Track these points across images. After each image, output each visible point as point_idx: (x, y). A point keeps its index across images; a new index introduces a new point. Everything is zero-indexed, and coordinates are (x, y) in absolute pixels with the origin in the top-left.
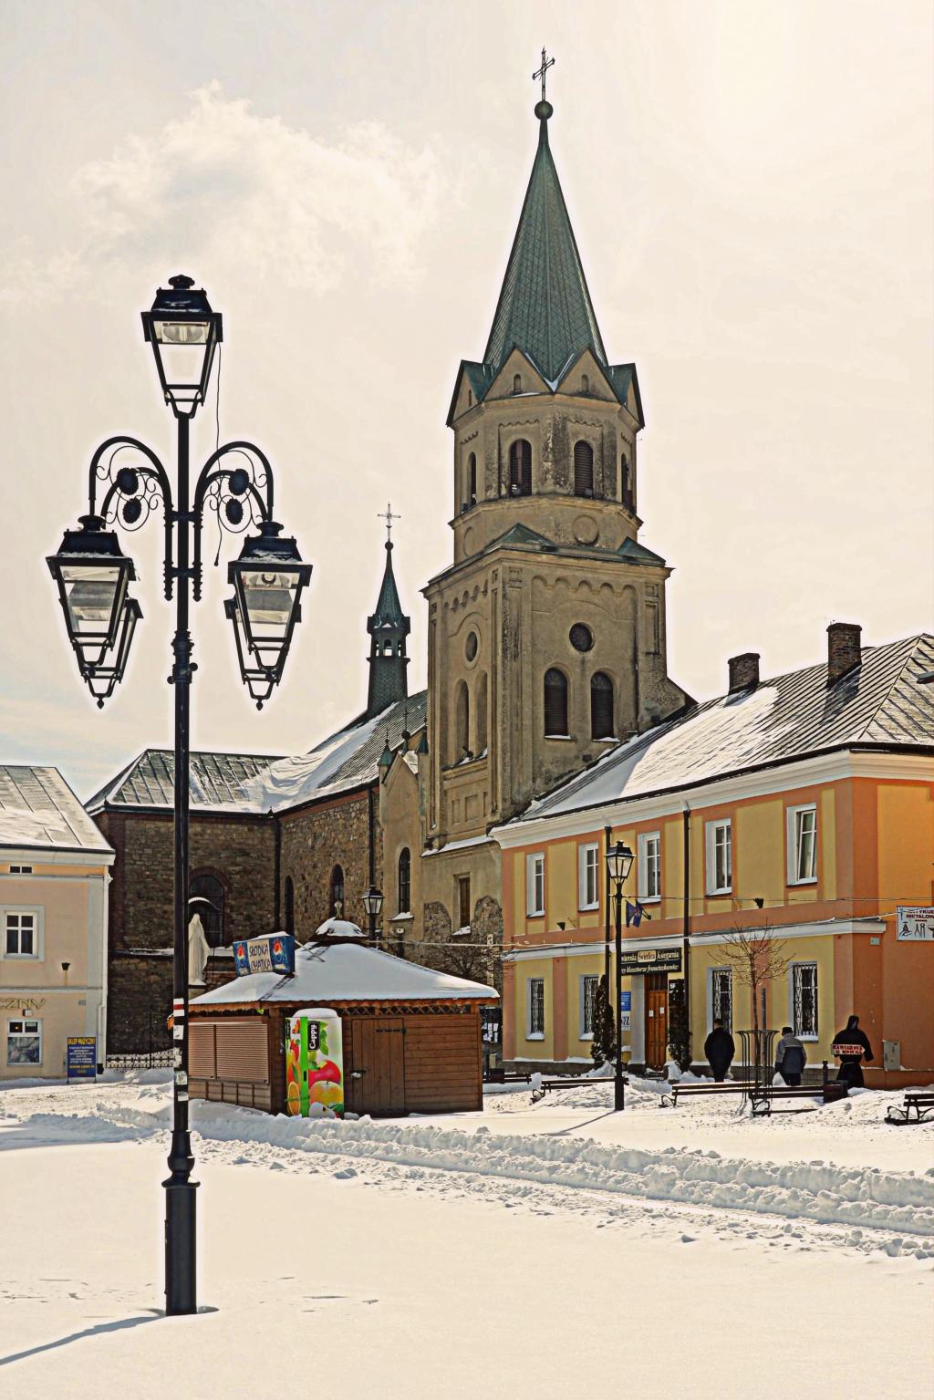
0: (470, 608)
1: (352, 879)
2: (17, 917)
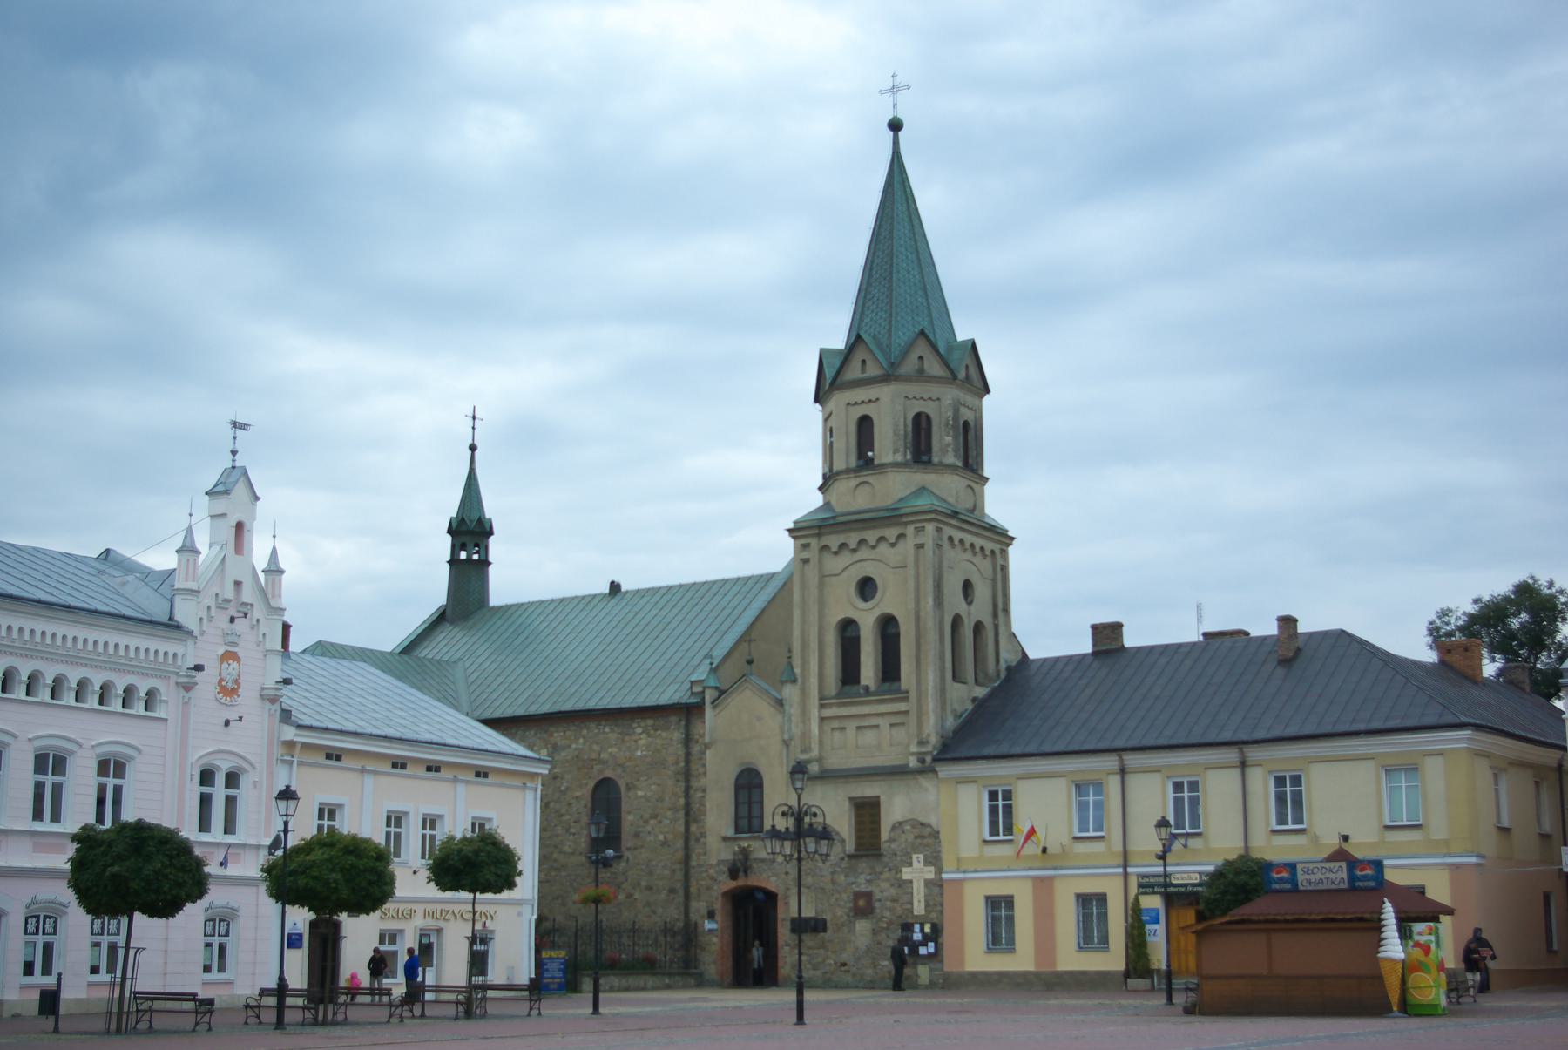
0: (864, 553)
2: (334, 820)
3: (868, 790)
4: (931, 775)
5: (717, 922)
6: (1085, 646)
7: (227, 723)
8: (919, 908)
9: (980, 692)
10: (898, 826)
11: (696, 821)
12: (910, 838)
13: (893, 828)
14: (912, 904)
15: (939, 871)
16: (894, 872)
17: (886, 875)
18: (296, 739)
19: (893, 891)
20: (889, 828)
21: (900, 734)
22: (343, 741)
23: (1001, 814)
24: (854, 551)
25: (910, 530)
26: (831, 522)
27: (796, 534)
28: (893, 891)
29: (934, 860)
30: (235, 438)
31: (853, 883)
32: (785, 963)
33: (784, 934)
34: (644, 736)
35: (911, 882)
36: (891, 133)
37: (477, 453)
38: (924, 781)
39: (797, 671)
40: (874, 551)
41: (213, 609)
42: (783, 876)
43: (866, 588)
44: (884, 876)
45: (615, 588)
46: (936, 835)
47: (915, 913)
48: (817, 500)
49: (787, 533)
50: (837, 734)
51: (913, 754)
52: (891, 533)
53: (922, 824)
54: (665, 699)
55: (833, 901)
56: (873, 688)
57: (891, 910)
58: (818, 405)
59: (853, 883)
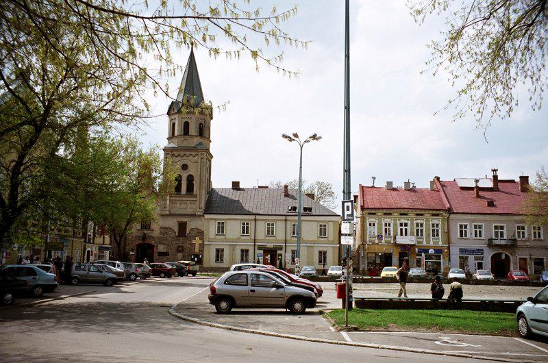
0: (185, 157)
3: (184, 220)
8: (197, 250)
10: (192, 229)
23: (221, 229)
25: (200, 153)
29: (202, 238)
43: (185, 167)
52: (194, 153)
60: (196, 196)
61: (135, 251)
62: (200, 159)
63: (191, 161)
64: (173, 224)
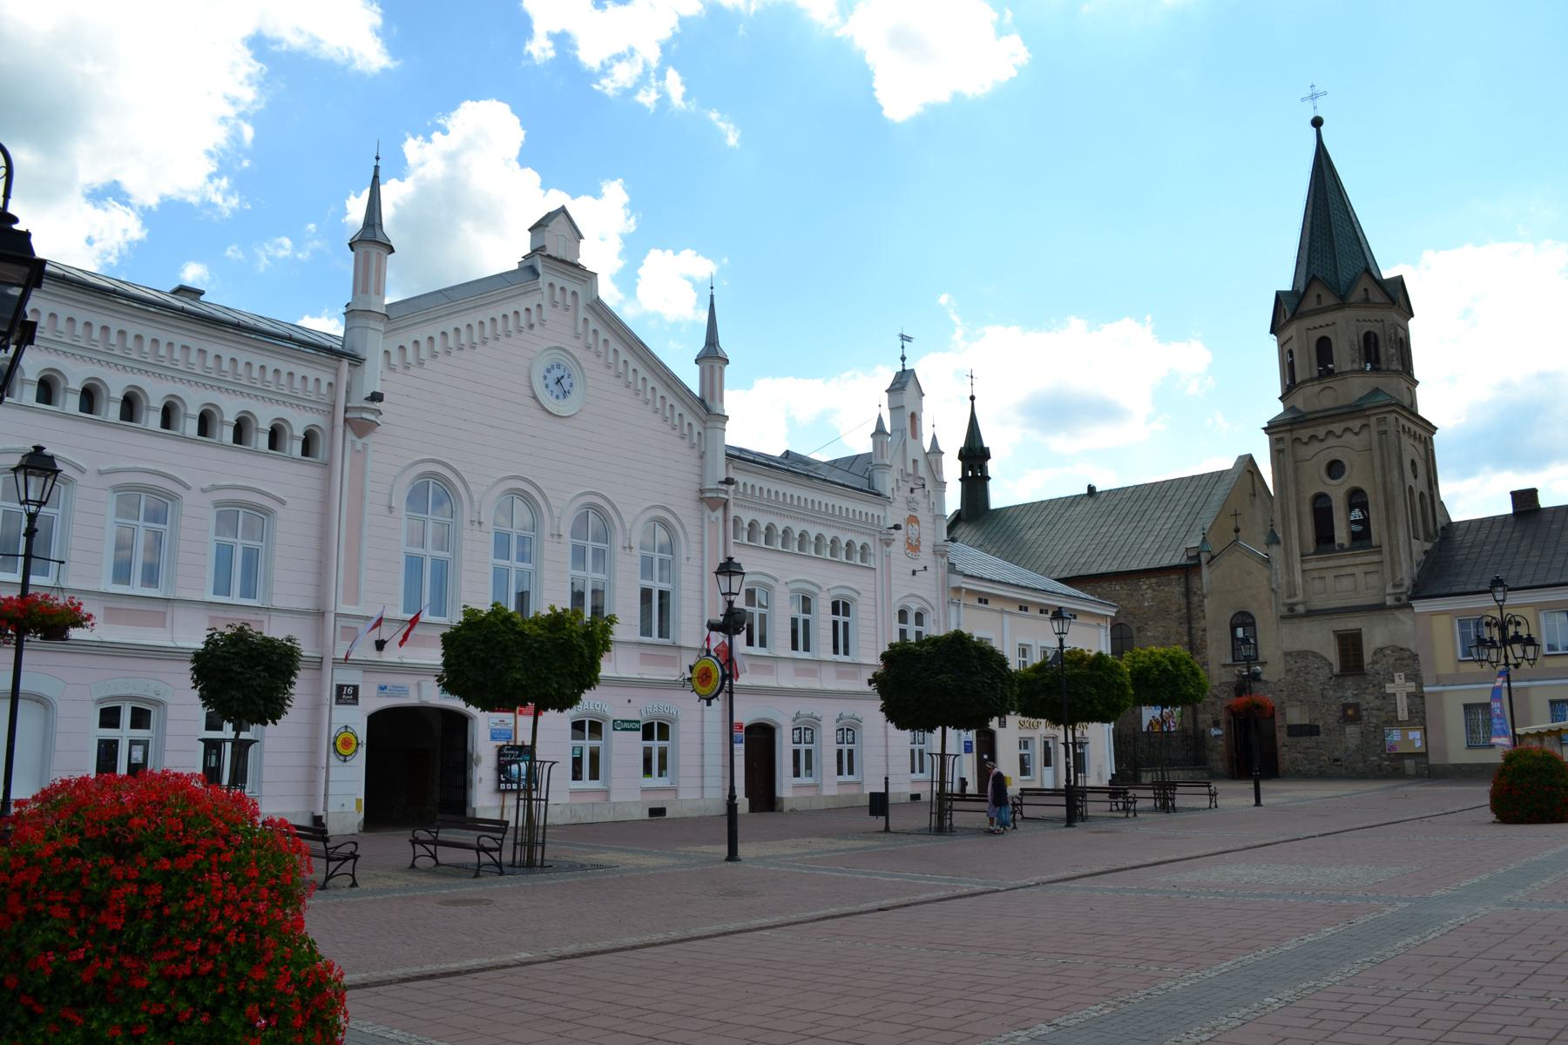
0: (1332, 441)
1: (1149, 634)
3: (1349, 624)
4: (1407, 610)
5: (1222, 729)
6: (1507, 508)
7: (914, 573)
8: (1403, 714)
9: (1428, 546)
11: (1198, 654)
12: (1392, 661)
13: (1375, 654)
14: (1396, 712)
15: (1420, 686)
16: (1377, 688)
17: (1371, 690)
18: (963, 586)
19: (1378, 703)
20: (1371, 653)
21: (1374, 580)
22: (992, 588)
24: (1322, 440)
25: (1373, 420)
26: (1302, 419)
27: (1269, 431)
28: (1378, 703)
29: (1415, 677)
30: (903, 347)
31: (1341, 697)
32: (1285, 759)
33: (1282, 736)
34: (1149, 591)
35: (1394, 694)
36: (1315, 129)
37: (975, 401)
38: (1399, 614)
39: (1280, 535)
40: (1339, 440)
41: (900, 482)
42: (1279, 693)
44: (1370, 691)
45: (1091, 489)
46: (1415, 657)
47: (1400, 719)
48: (1279, 408)
49: (1263, 431)
50: (1317, 582)
51: (1389, 595)
52: (1355, 424)
53: (1401, 649)
54: (1165, 563)
55: (1323, 711)
56: (1347, 545)
57: (1378, 717)
58: (1273, 336)
59: (1341, 697)
60: (1378, 549)
61: (1223, 725)
62: (1375, 436)
63: (1350, 446)
64: (1320, 639)
